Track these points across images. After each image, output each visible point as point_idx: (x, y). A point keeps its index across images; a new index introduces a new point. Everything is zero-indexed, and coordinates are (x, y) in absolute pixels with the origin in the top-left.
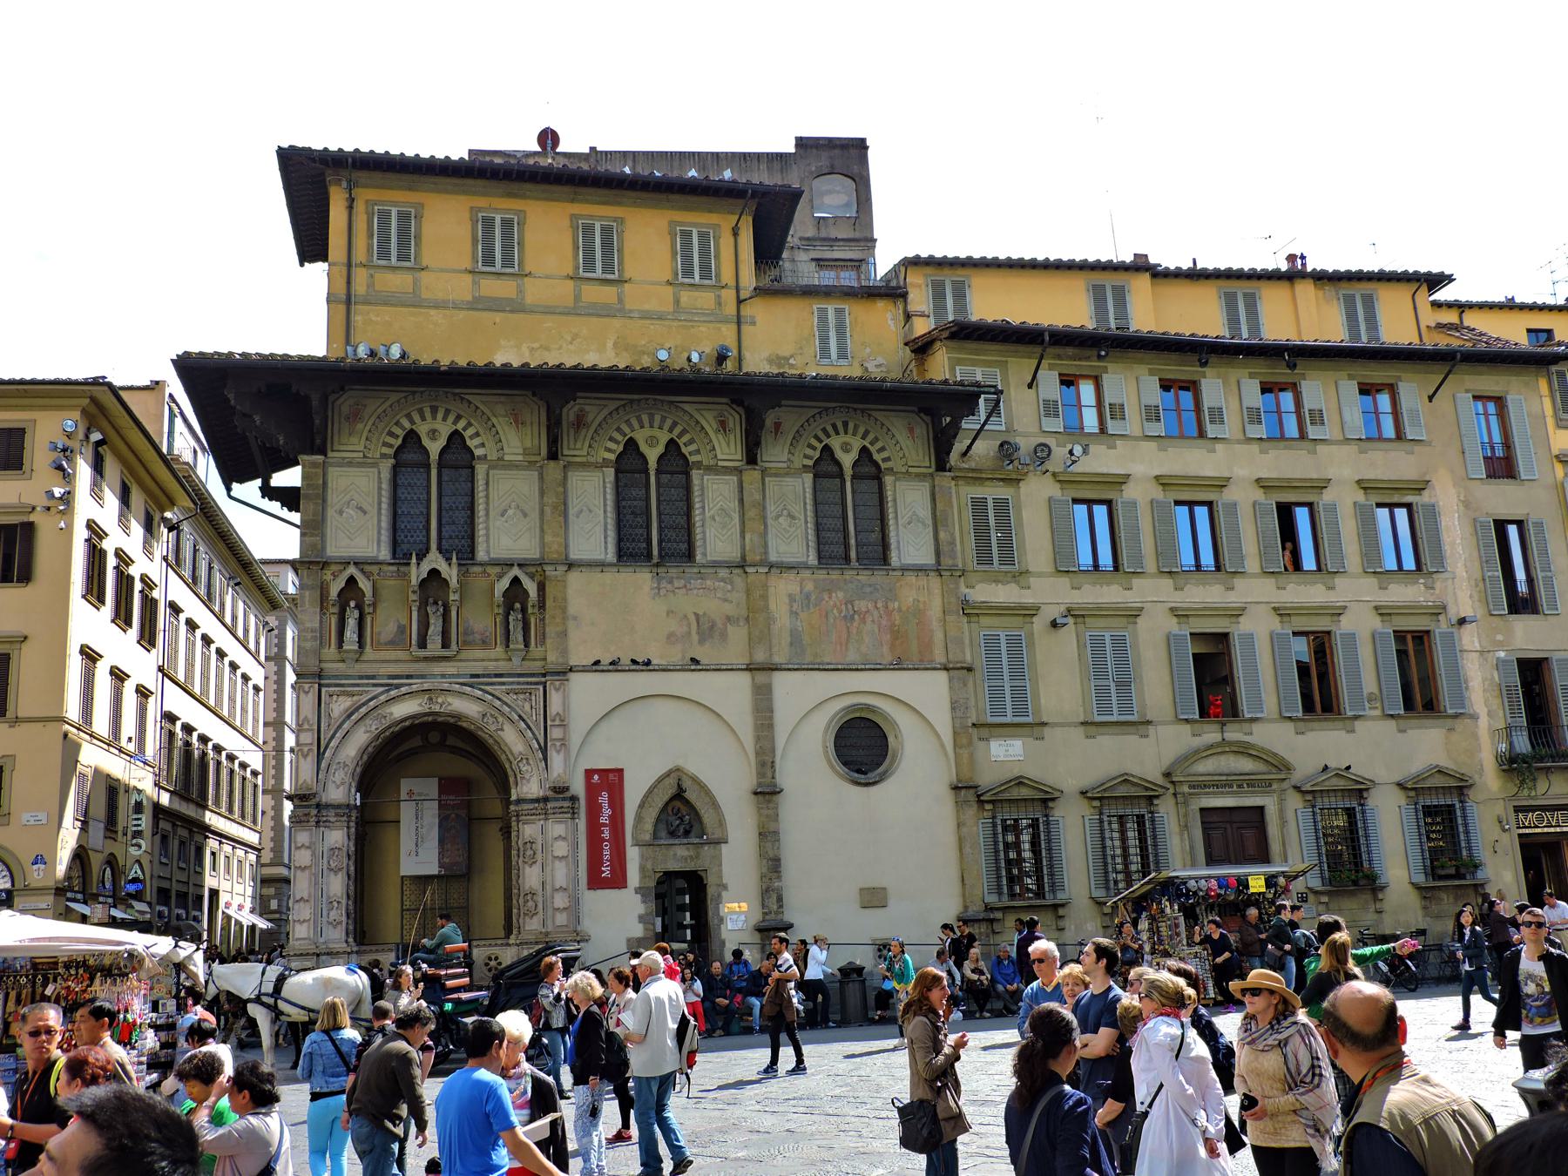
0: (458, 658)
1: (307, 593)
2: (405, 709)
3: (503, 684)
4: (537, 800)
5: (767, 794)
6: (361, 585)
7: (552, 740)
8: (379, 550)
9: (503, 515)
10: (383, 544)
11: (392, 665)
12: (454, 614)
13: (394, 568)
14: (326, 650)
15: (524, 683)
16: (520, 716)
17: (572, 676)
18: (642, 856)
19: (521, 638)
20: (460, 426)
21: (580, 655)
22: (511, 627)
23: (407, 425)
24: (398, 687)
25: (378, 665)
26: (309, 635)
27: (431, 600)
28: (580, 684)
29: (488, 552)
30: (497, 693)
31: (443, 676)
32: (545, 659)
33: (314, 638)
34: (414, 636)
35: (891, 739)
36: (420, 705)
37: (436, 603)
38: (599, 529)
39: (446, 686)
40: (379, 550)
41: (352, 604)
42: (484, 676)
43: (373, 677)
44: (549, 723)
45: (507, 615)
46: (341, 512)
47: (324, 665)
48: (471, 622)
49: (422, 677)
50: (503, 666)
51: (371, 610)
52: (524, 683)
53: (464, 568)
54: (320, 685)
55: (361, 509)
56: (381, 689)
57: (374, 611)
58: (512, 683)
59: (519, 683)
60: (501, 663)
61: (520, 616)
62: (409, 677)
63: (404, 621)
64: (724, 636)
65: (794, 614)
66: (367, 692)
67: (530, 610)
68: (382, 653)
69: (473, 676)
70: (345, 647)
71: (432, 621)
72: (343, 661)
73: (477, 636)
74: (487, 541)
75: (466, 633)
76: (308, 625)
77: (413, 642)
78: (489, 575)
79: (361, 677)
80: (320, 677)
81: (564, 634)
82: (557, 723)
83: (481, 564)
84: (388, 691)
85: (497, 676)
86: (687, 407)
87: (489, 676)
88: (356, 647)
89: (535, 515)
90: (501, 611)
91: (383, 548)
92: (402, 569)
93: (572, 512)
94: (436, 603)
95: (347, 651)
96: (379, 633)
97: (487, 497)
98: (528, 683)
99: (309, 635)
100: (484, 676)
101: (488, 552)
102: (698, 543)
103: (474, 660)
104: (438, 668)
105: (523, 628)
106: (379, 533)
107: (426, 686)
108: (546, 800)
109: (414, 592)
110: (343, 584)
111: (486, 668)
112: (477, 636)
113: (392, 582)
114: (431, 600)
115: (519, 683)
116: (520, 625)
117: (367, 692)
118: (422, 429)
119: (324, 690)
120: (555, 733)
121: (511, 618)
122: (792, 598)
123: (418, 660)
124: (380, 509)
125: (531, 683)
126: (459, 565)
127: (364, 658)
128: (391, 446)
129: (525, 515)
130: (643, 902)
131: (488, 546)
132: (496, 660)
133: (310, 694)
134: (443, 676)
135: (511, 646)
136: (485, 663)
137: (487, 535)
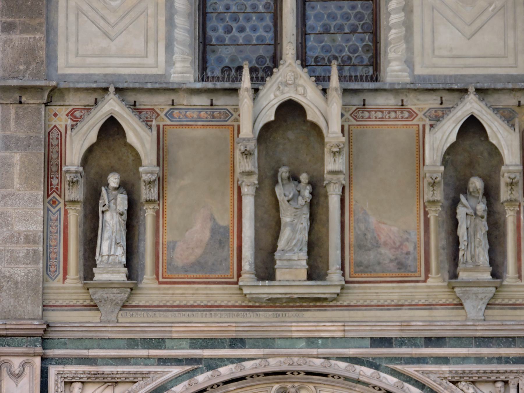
0: (345, 301)
1: (17, 157)
3: (445, 360)
6: (131, 138)
8: (170, 62)
10: (177, 48)
11: (199, 316)
12: (334, 201)
13: (203, 101)
14: (56, 283)
15: (490, 360)
19: (483, 258)
22: (462, 232)
25: (169, 317)
26: (22, 250)
27: (284, 172)
29: (409, 63)
31: (311, 342)
33: (33, 256)
34: (248, 252)
37: (294, 178)
39: (317, 365)
40: (170, 62)
41: (113, 180)
42: (402, 342)
45: (455, 202)
47: (54, 316)
48: (373, 220)
51: (153, 194)
52: (490, 360)
53: (356, 100)
54: (44, 359)
56: (175, 370)
57: (161, 194)
58: (464, 359)
59: (479, 360)
60: (440, 314)
61: (482, 207)
66: (145, 376)
67: (504, 194)
68: (179, 289)
70: (100, 276)
71: (286, 219)
72: (95, 307)
73: (387, 253)
74: (408, 37)
75: (361, 247)
76: (20, 227)
77: (246, 266)
78: (412, 115)
79: (133, 343)
80: (45, 341)
83: (394, 91)
84: (190, 374)
85: (430, 341)
87: (411, 342)
88: (121, 276)
90: (439, 195)
91: (177, 57)
92: (221, 101)
94: (294, 178)
95: (106, 285)
96: (172, 246)
98: (500, 360)
99: (22, 250)
100: (402, 342)
101: (409, 63)
103: (380, 307)
105: (489, 234)
106: (170, 23)
107: (274, 365)
109: (246, 154)
110: (92, 138)
111: (405, 324)
112: (387, 253)
113: (199, 133)
114: (284, 172)
115: (479, 360)
116: (483, 226)
117: (145, 376)
119: (53, 371)
121: (461, 212)
125: (507, 360)
126: (345, 91)
127: (140, 300)
131: (410, 49)
132: (429, 306)
133: (24, 381)
134: (311, 342)
135: (463, 275)
136: (405, 314)
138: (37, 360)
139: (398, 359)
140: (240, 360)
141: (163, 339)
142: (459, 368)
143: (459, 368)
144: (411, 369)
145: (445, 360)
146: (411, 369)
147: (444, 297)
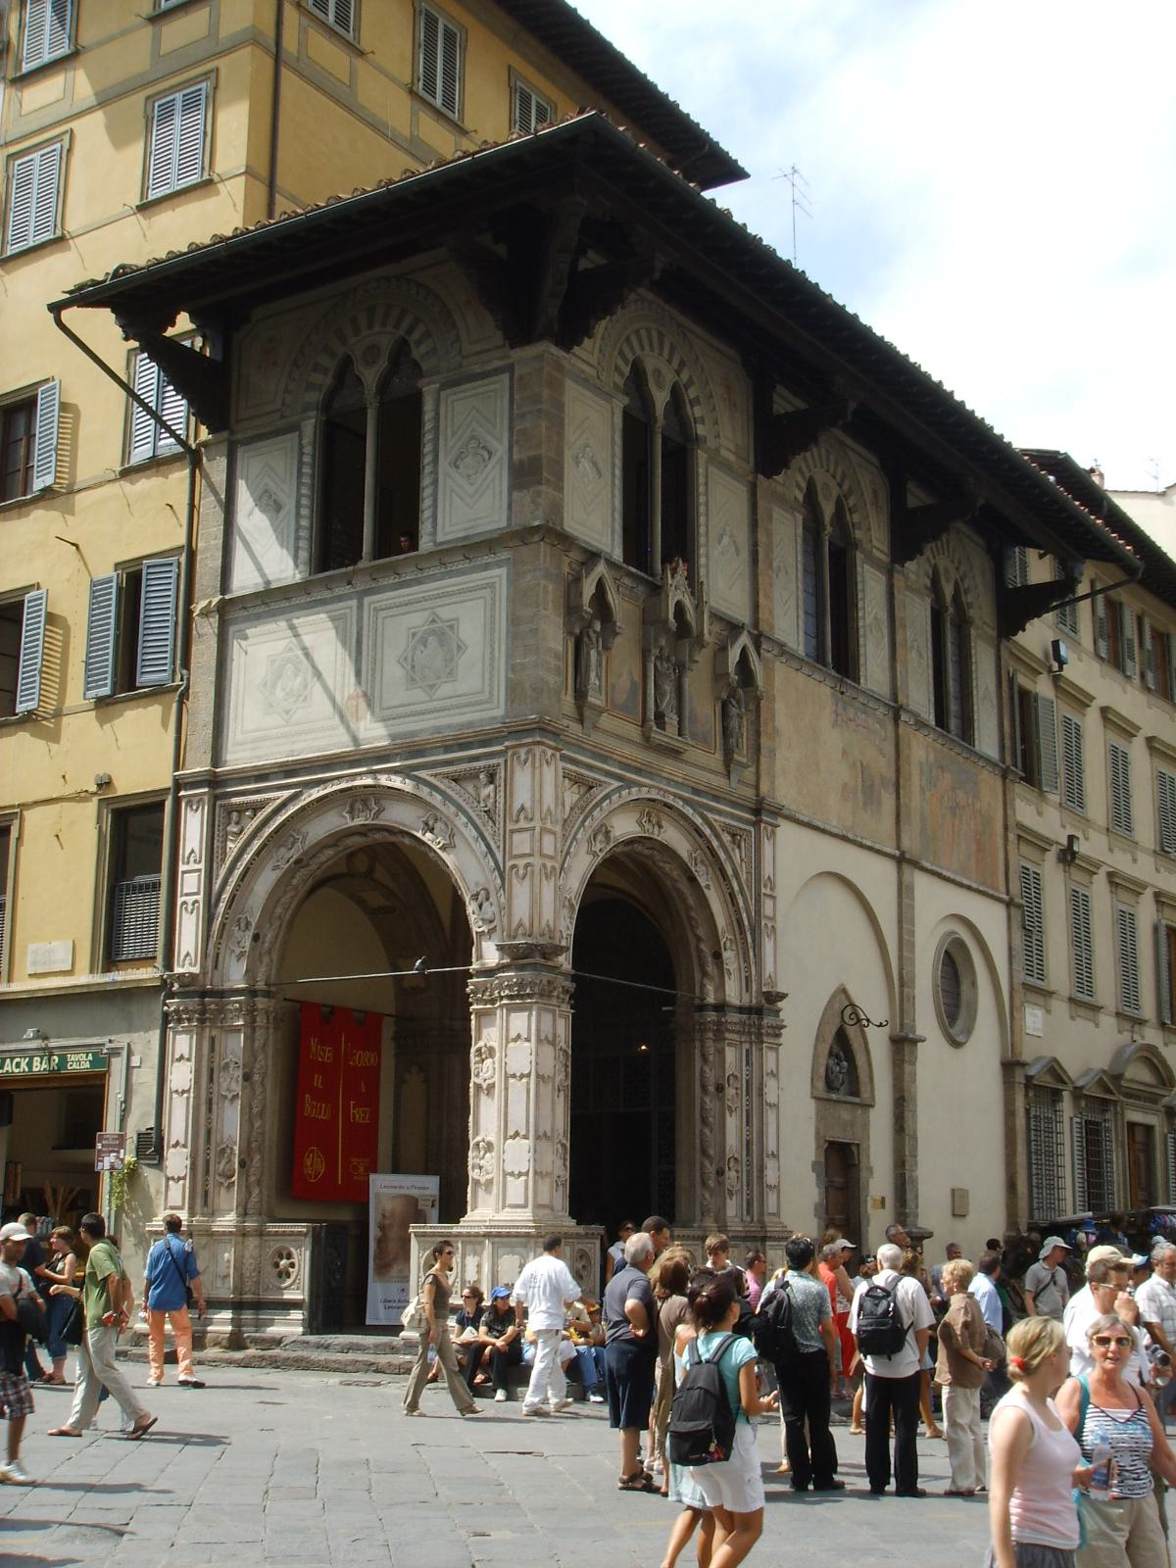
1: (551, 587)
2: (625, 827)
3: (720, 813)
4: (741, 1010)
5: (903, 1044)
7: (766, 917)
9: (720, 543)
16: (735, 870)
17: (780, 821)
18: (820, 1117)
20: (685, 376)
21: (784, 790)
23: (638, 351)
24: (629, 784)
28: (786, 831)
30: (715, 824)
32: (757, 787)
35: (965, 987)
36: (640, 823)
38: (792, 602)
39: (670, 800)
43: (604, 759)
44: (763, 890)
46: (578, 463)
49: (650, 775)
50: (718, 782)
55: (595, 464)
56: (616, 784)
62: (638, 771)
63: (637, 678)
64: (879, 803)
65: (922, 790)
66: (600, 784)
69: (696, 792)
81: (773, 752)
82: (768, 892)
84: (619, 789)
86: (851, 454)
89: (745, 555)
93: (775, 564)
97: (707, 502)
99: (553, 662)
102: (862, 661)
104: (669, 766)
107: (654, 795)
108: (758, 1011)
118: (650, 364)
120: (767, 907)
122: (921, 763)
123: (647, 743)
124: (613, 473)
128: (621, 374)
129: (737, 551)
130: (818, 1186)
137: (707, 566)
138: (558, 754)
139: (712, 810)
140: (641, 785)
141: (607, 757)
142: (728, 821)
143: (728, 821)
144: (709, 815)
145: (720, 813)
146: (709, 815)
147: (721, 768)
